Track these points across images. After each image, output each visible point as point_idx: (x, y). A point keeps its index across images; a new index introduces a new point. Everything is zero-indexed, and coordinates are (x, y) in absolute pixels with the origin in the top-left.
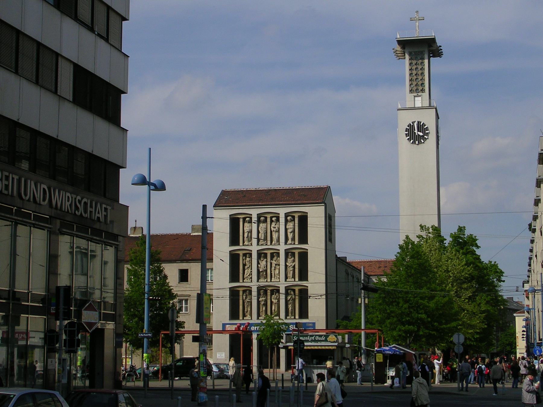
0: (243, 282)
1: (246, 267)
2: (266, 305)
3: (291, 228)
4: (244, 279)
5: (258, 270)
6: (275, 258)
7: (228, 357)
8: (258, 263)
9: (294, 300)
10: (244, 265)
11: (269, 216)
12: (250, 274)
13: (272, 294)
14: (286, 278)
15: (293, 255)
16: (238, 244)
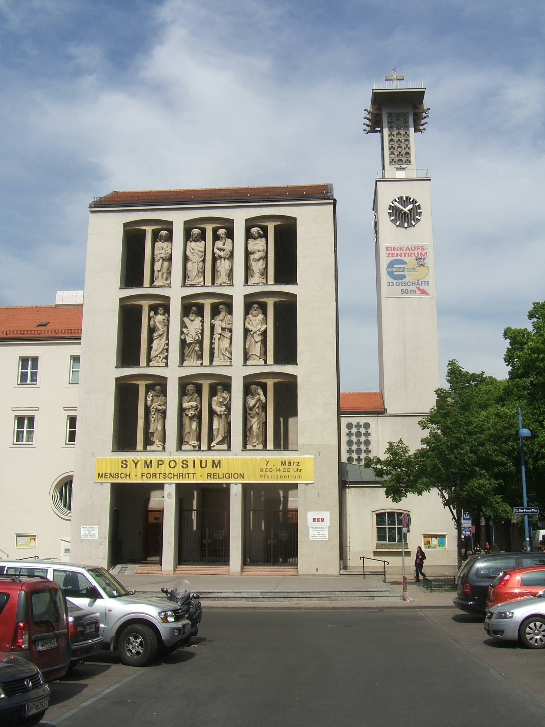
0: (148, 365)
1: (156, 335)
2: (199, 417)
4: (149, 360)
5: (183, 343)
6: (223, 314)
7: (105, 538)
8: (183, 325)
9: (264, 407)
10: (152, 330)
12: (163, 349)
13: (213, 393)
14: (246, 357)
15: (263, 307)
16: (139, 283)
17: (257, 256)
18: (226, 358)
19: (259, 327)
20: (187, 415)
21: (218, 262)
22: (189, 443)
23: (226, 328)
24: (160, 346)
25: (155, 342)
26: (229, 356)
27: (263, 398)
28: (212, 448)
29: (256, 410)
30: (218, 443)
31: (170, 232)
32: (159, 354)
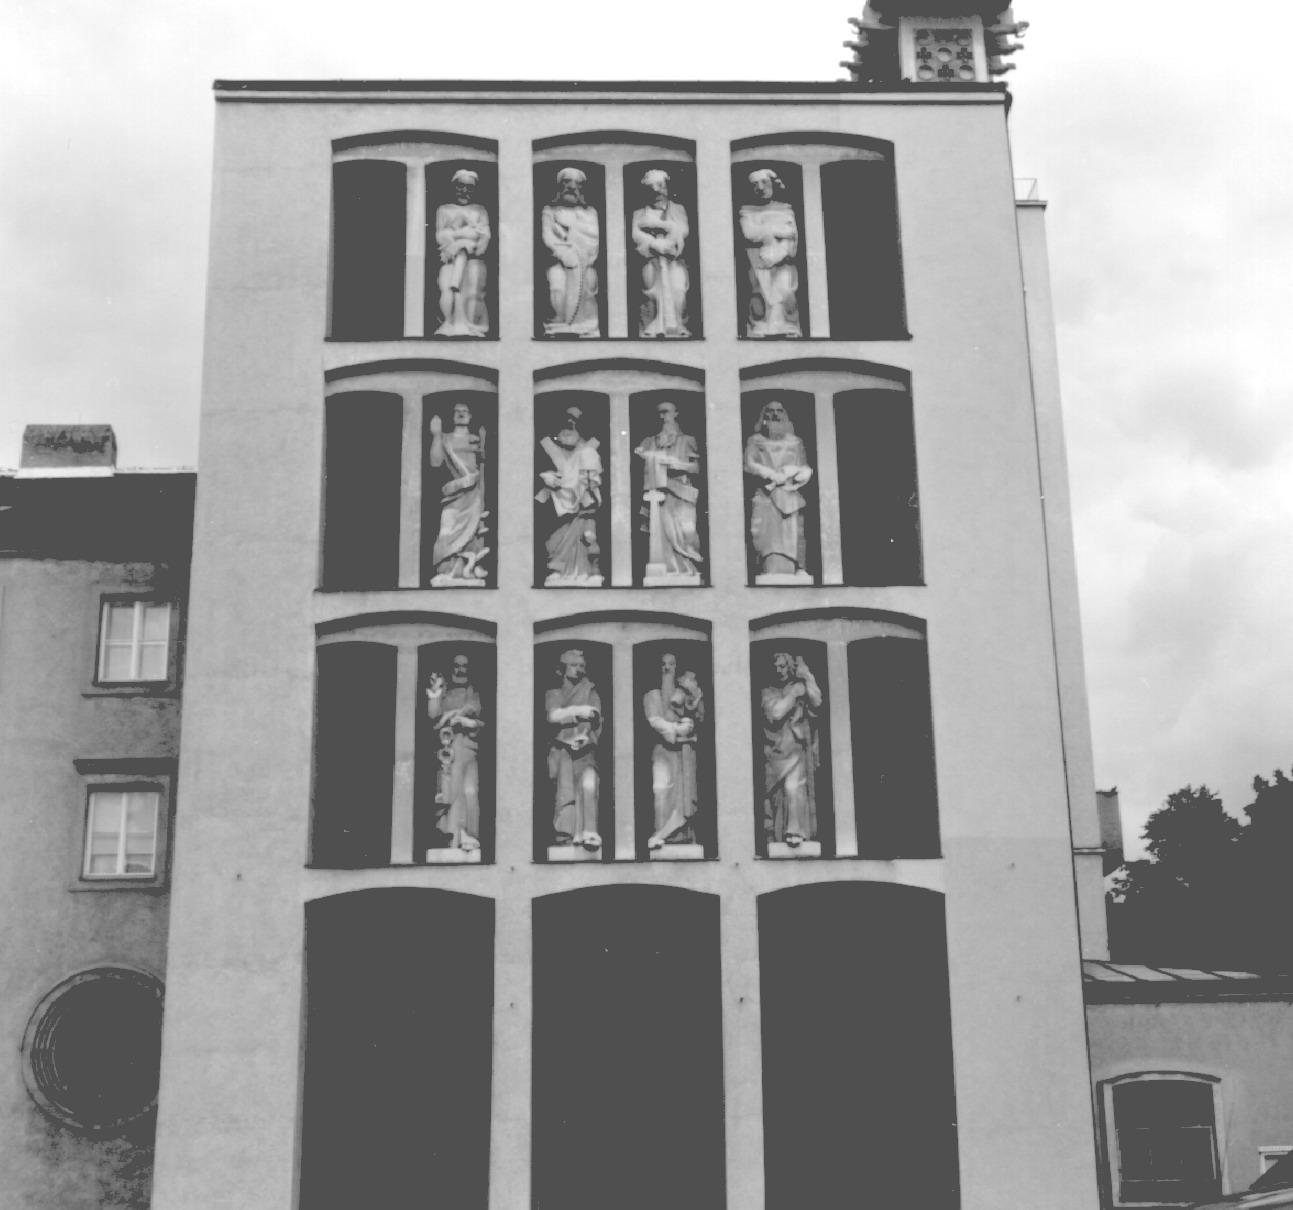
0: (425, 585)
2: (601, 755)
3: (779, 239)
4: (429, 569)
8: (543, 462)
9: (818, 718)
11: (614, 161)
12: (477, 535)
13: (647, 676)
14: (756, 563)
15: (801, 409)
17: (775, 252)
18: (687, 563)
19: (790, 470)
20: (561, 745)
21: (649, 271)
22: (572, 838)
23: (681, 473)
24: (465, 528)
25: (448, 515)
26: (698, 558)
27: (814, 691)
28: (653, 854)
29: (797, 730)
30: (669, 841)
31: (489, 174)
32: (464, 549)
